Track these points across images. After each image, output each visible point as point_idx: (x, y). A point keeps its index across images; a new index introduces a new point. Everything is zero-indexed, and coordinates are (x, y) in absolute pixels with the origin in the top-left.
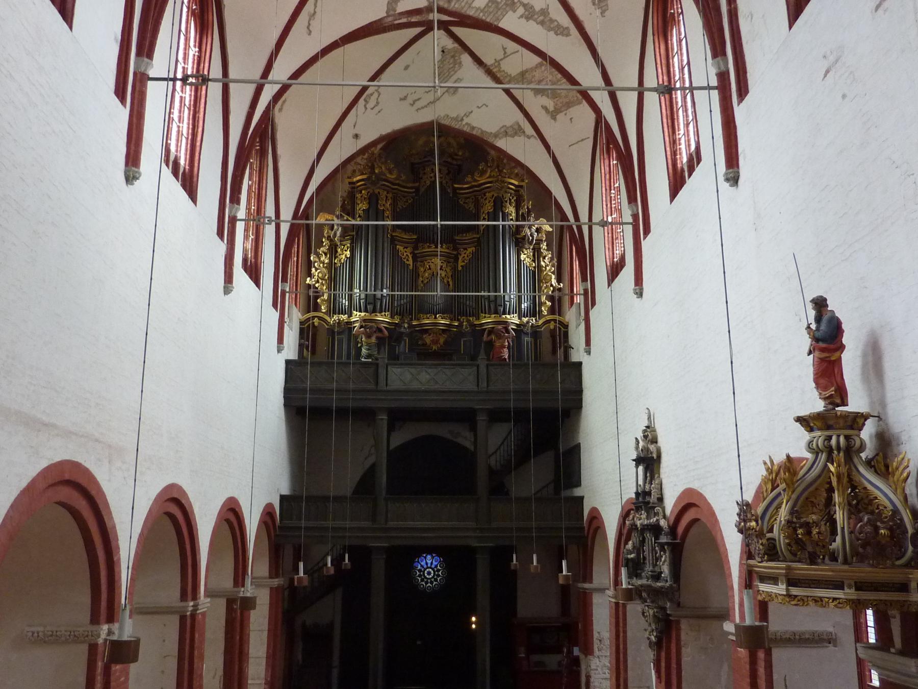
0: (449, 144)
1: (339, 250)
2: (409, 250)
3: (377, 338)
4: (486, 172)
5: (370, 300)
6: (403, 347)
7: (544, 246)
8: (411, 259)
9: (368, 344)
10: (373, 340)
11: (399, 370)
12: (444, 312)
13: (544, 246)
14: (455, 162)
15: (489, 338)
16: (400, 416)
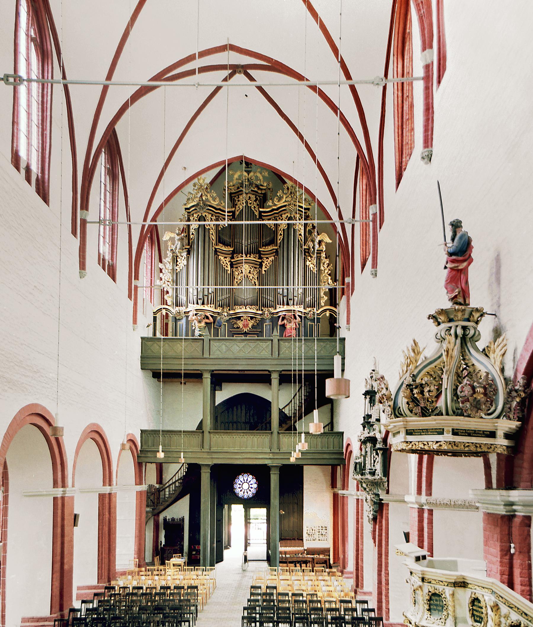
0: (257, 178)
1: (178, 260)
2: (228, 259)
3: (206, 323)
4: (283, 197)
5: (200, 296)
6: (224, 329)
7: (323, 255)
8: (229, 266)
9: (199, 327)
10: (203, 324)
12: (252, 304)
13: (323, 255)
14: (260, 192)
15: (283, 322)
16: (219, 380)
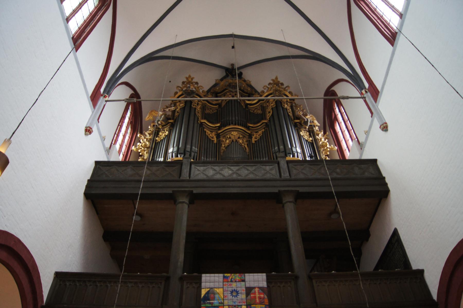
11: (202, 168)
